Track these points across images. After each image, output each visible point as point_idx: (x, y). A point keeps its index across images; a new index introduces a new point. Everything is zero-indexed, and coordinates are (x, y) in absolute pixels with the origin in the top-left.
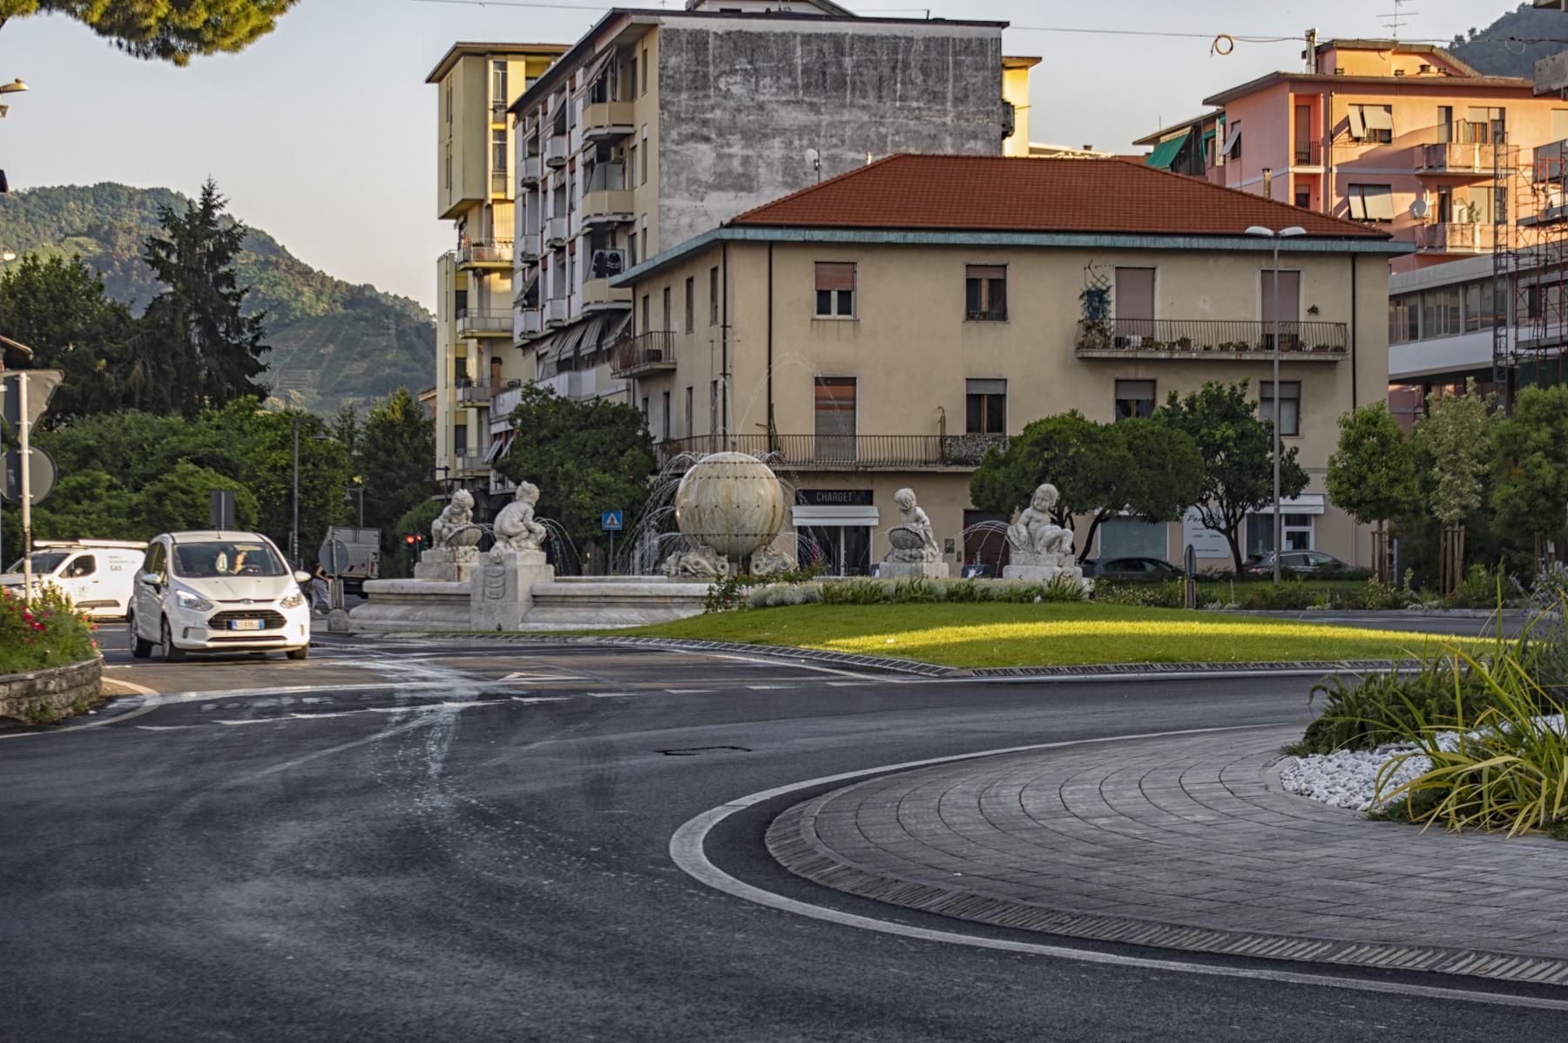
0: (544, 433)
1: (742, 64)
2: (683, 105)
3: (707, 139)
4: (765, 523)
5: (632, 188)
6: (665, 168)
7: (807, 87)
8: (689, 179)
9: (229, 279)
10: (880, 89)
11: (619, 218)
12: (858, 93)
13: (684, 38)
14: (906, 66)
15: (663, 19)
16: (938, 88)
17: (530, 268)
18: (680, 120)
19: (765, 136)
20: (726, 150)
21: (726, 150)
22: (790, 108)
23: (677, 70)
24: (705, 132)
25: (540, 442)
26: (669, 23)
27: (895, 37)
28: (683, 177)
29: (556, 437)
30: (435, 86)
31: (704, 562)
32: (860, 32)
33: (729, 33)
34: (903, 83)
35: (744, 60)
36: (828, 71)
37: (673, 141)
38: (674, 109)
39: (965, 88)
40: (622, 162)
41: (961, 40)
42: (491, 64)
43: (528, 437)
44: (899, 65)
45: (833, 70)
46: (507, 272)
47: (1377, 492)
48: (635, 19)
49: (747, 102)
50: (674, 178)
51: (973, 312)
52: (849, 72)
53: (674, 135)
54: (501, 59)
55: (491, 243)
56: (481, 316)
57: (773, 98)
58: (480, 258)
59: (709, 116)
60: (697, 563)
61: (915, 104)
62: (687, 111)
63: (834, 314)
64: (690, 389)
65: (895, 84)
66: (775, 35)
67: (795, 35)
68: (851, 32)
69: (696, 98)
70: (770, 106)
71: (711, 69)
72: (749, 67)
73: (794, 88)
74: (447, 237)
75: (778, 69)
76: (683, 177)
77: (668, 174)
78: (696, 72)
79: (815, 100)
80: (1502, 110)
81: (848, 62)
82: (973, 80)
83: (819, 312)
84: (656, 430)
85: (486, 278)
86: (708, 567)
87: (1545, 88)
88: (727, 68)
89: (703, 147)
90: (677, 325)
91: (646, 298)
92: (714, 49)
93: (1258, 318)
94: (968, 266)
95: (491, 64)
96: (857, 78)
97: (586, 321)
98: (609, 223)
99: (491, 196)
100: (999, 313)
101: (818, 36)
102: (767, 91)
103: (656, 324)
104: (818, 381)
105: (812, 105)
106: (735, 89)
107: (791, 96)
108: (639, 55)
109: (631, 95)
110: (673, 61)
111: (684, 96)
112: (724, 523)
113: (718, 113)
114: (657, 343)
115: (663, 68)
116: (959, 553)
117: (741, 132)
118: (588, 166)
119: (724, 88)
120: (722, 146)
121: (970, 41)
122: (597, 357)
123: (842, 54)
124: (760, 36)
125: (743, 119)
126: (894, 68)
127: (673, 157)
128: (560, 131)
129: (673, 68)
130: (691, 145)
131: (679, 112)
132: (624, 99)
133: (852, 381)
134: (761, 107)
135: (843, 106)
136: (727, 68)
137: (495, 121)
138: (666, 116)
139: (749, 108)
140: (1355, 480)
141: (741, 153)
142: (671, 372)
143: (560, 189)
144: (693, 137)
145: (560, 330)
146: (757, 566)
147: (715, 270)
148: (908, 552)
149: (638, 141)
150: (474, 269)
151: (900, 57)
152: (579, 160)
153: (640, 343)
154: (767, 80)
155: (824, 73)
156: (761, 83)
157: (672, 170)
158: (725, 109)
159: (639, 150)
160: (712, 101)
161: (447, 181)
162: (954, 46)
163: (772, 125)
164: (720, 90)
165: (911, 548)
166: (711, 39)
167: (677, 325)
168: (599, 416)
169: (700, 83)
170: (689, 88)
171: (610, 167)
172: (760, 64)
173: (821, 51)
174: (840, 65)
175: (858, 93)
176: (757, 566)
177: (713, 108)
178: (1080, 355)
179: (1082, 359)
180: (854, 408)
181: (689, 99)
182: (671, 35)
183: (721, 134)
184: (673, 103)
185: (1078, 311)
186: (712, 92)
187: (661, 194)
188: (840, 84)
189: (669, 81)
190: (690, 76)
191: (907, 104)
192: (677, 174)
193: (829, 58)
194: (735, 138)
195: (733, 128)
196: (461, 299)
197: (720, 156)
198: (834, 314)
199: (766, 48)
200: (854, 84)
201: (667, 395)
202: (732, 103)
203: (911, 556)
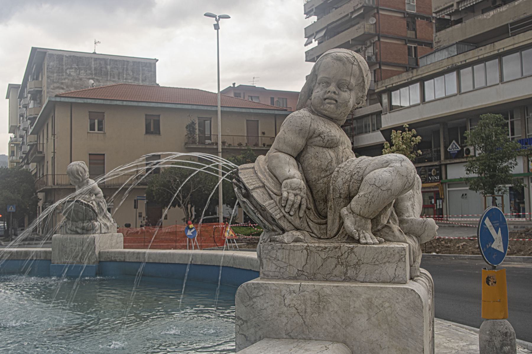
1: (75, 66)
2: (55, 77)
7: (95, 74)
10: (119, 76)
12: (112, 77)
13: (55, 57)
14: (127, 70)
15: (48, 50)
16: (137, 77)
18: (54, 82)
24: (62, 86)
26: (50, 52)
27: (124, 61)
30: (8, 100)
33: (70, 56)
34: (126, 75)
36: (103, 69)
37: (51, 89)
39: (145, 77)
41: (144, 63)
44: (125, 69)
49: (76, 78)
51: (148, 131)
52: (109, 70)
53: (52, 87)
57: (85, 77)
59: (63, 81)
63: (96, 131)
65: (124, 74)
67: (92, 58)
68: (110, 58)
69: (59, 76)
70: (84, 79)
72: (77, 67)
73: (91, 74)
78: (59, 67)
79: (98, 78)
81: (109, 67)
82: (148, 75)
83: (91, 130)
92: (65, 61)
93: (246, 135)
94: (146, 115)
96: (111, 72)
100: (157, 131)
101: (99, 59)
104: (90, 154)
105: (97, 80)
106: (72, 73)
107: (90, 77)
110: (51, 63)
111: (55, 75)
113: (66, 81)
114: (41, 150)
115: (48, 66)
116: (144, 217)
117: (74, 87)
119: (69, 73)
121: (147, 63)
123: (107, 65)
124: (80, 58)
125: (75, 83)
126: (123, 70)
131: (53, 80)
133: (104, 155)
134: (81, 79)
135: (107, 80)
136: (70, 67)
138: (49, 80)
139: (76, 79)
148: (80, 225)
151: (125, 67)
154: (83, 71)
155: (101, 70)
156: (81, 72)
158: (69, 80)
160: (64, 77)
162: (142, 64)
164: (67, 73)
165: (83, 221)
166: (64, 58)
172: (80, 66)
174: (106, 68)
175: (112, 77)
177: (65, 79)
178: (186, 147)
179: (187, 148)
180: (104, 164)
181: (57, 76)
182: (51, 55)
183: (67, 87)
184: (52, 77)
185: (185, 132)
186: (64, 74)
189: (50, 70)
190: (57, 69)
191: (128, 81)
193: (102, 66)
198: (96, 131)
200: (111, 74)
202: (71, 78)
203: (83, 228)
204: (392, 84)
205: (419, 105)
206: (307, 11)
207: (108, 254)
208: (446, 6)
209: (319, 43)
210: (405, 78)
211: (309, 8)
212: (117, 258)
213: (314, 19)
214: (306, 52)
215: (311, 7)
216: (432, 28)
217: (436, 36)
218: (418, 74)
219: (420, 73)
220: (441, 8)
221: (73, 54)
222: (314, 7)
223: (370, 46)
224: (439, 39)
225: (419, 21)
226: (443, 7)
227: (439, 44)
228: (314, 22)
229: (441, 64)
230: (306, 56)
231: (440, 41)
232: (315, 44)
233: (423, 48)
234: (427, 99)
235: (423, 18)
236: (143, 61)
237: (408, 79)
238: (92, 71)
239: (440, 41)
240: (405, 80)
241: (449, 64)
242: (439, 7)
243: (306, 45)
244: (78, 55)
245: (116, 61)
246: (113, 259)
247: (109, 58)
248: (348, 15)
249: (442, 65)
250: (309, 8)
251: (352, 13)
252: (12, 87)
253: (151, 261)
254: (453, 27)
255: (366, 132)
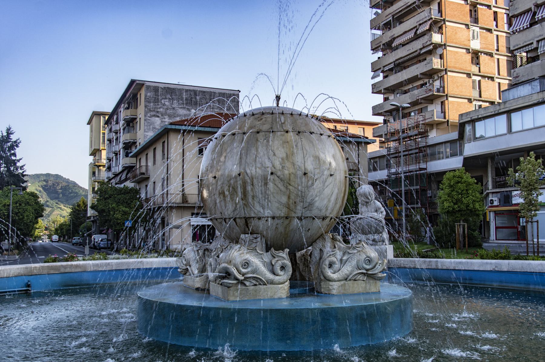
0: (107, 196)
1: (169, 96)
3: (158, 117)
4: (337, 199)
5: (136, 133)
6: (146, 124)
7: (187, 104)
8: (153, 128)
9: (14, 155)
11: (132, 141)
13: (152, 88)
15: (146, 82)
17: (110, 162)
18: (150, 111)
19: (175, 116)
20: (164, 120)
21: (164, 120)
22: (182, 109)
23: (150, 97)
24: (158, 114)
25: (105, 199)
26: (148, 84)
27: (211, 92)
28: (151, 127)
29: (110, 197)
30: (89, 126)
31: (256, 261)
32: (201, 90)
35: (169, 95)
38: (149, 108)
40: (133, 127)
42: (102, 117)
43: (102, 198)
45: (194, 100)
46: (104, 166)
47: (468, 206)
48: (137, 82)
50: (149, 127)
53: (149, 115)
54: (104, 116)
55: (101, 159)
56: (98, 177)
58: (98, 162)
59: (159, 110)
60: (246, 264)
61: (216, 110)
62: (153, 108)
64: (154, 183)
66: (178, 89)
67: (183, 89)
70: (176, 108)
71: (160, 97)
73: (183, 104)
74: (91, 159)
75: (179, 98)
76: (151, 127)
77: (147, 126)
78: (155, 98)
80: (347, 127)
81: (198, 98)
84: (143, 196)
85: (100, 168)
86: (263, 269)
87: (377, 112)
88: (164, 97)
89: (157, 119)
90: (150, 163)
91: (140, 159)
95: (102, 117)
96: (200, 102)
97: (123, 171)
98: (130, 142)
99: (101, 148)
101: (190, 90)
102: (175, 105)
103: (143, 163)
105: (188, 108)
106: (167, 103)
108: (139, 96)
109: (136, 108)
110: (149, 94)
111: (152, 104)
112: (284, 199)
113: (161, 110)
115: (146, 96)
118: (124, 129)
120: (162, 119)
122: (126, 180)
124: (174, 89)
125: (168, 111)
127: (148, 121)
128: (117, 123)
129: (149, 96)
130: (153, 118)
131: (150, 109)
132: (134, 108)
134: (174, 108)
136: (164, 97)
137: (103, 130)
138: (146, 109)
140: (455, 201)
141: (168, 121)
142: (148, 179)
143: (117, 139)
144: (154, 116)
145: (116, 175)
146: (331, 266)
147: (164, 142)
149: (138, 120)
150: (96, 165)
152: (122, 128)
153: (138, 172)
154: (176, 101)
157: (148, 125)
158: (163, 108)
159: (138, 123)
160: (160, 106)
161: (91, 146)
163: (177, 114)
166: (160, 89)
167: (150, 163)
168: (127, 191)
169: (156, 101)
170: (153, 102)
171: (130, 128)
172: (174, 97)
173: (190, 94)
174: (196, 99)
176: (331, 266)
177: (160, 108)
182: (148, 87)
183: (162, 115)
184: (148, 106)
187: (145, 131)
188: (196, 104)
190: (154, 99)
192: (149, 126)
193: (193, 96)
194: (166, 117)
195: (166, 114)
196: (94, 173)
197: (162, 122)
199: (175, 92)
200: (199, 104)
201: (147, 186)
203: (374, 240)
204: (478, 116)
205: (505, 134)
206: (374, 48)
207: (398, 262)
208: (525, 44)
209: (385, 77)
210: (492, 110)
211: (376, 45)
212: (406, 266)
213: (380, 54)
214: (372, 85)
215: (378, 44)
216: (494, 62)
217: (515, 71)
218: (506, 107)
219: (508, 106)
220: (519, 46)
221: (167, 86)
222: (381, 44)
223: (438, 79)
224: (517, 74)
225: (483, 57)
226: (522, 45)
227: (517, 79)
228: (379, 58)
229: (531, 98)
230: (373, 89)
231: (519, 76)
232: (380, 78)
233: (486, 81)
234: (514, 130)
235: (486, 54)
236: (227, 92)
237: (495, 112)
238: (183, 101)
239: (519, 76)
240: (492, 112)
241: (539, 98)
242: (518, 45)
243: (372, 78)
244: (172, 86)
245: (204, 92)
246: (402, 266)
247: (199, 89)
248: (417, 51)
249: (531, 99)
250: (376, 45)
251: (421, 49)
252: (95, 114)
253: (445, 268)
254: (532, 63)
255: (439, 159)
